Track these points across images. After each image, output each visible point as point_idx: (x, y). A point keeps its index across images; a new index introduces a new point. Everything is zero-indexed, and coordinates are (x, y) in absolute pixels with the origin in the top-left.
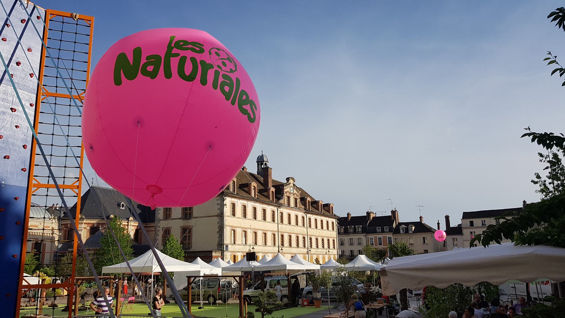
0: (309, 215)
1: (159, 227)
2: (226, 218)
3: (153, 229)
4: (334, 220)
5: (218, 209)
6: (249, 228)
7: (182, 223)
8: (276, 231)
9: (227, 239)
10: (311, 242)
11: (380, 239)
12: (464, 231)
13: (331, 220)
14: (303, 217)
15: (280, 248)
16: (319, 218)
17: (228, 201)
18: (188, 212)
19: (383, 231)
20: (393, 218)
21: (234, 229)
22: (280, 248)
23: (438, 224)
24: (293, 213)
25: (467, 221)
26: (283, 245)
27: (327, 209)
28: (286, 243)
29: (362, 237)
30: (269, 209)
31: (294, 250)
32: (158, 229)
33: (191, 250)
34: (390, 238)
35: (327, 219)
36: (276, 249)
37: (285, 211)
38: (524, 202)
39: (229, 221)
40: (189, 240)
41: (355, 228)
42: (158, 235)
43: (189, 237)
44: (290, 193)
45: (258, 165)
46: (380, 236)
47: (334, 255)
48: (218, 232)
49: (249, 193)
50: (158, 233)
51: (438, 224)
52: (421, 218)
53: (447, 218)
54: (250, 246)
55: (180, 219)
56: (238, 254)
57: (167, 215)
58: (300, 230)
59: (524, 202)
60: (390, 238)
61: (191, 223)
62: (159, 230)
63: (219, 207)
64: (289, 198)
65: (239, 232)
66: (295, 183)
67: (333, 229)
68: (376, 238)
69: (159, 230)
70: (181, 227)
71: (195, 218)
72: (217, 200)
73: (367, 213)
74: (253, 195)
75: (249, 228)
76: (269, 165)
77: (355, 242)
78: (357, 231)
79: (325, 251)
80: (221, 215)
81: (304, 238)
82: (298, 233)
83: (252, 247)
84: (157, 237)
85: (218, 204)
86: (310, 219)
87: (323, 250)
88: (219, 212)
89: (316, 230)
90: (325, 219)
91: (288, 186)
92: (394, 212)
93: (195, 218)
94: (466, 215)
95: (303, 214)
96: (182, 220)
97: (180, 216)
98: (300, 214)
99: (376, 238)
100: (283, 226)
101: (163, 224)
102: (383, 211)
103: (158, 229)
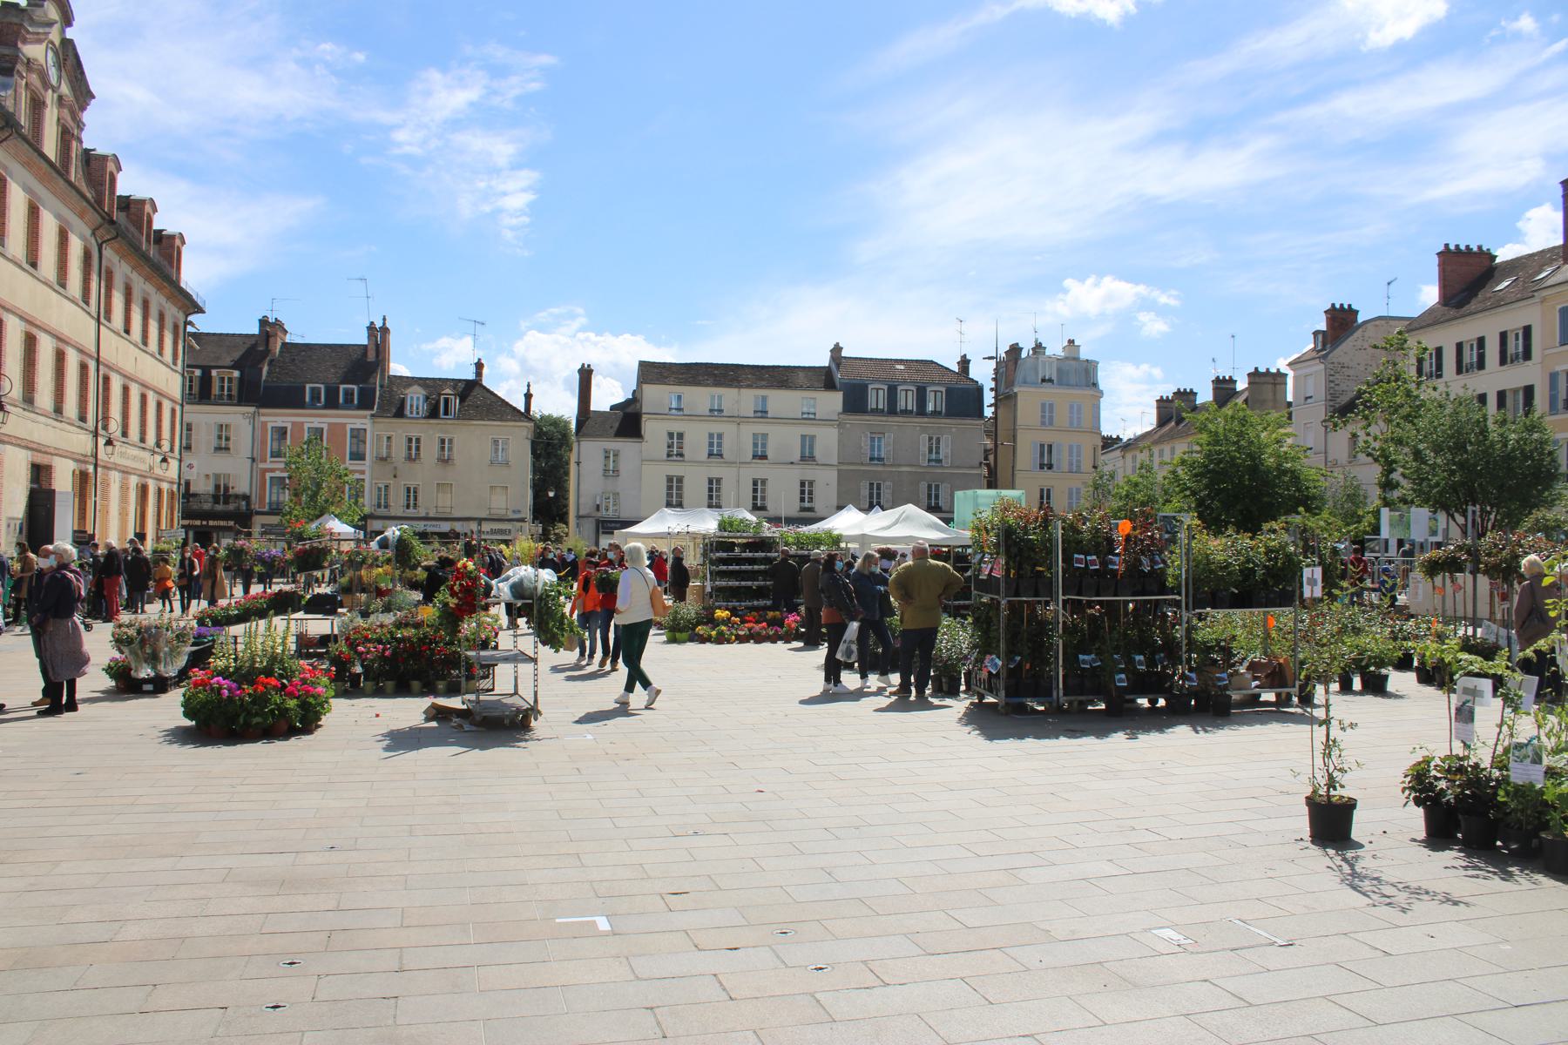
12: (649, 426)
19: (332, 403)
20: (371, 357)
25: (657, 395)
29: (238, 418)
34: (358, 435)
38: (837, 350)
51: (528, 396)
52: (479, 366)
53: (586, 375)
59: (837, 350)
60: (358, 435)
77: (204, 439)
78: (216, 390)
92: (379, 335)
94: (651, 372)
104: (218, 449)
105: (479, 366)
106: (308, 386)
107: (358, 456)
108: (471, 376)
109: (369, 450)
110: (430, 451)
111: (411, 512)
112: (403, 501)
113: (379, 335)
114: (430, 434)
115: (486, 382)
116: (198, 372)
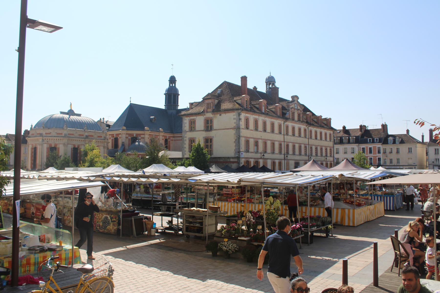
0: (310, 128)
1: (186, 137)
2: (242, 130)
3: (180, 138)
4: (332, 132)
5: (235, 123)
6: (260, 139)
7: (205, 134)
8: (282, 142)
9: (243, 148)
10: (312, 150)
11: (370, 148)
13: (329, 132)
14: (305, 130)
15: (286, 156)
16: (319, 130)
17: (243, 115)
18: (209, 125)
19: (373, 142)
21: (247, 139)
22: (286, 156)
23: (423, 136)
24: (297, 126)
26: (288, 153)
27: (325, 123)
28: (291, 152)
29: (355, 146)
30: (277, 122)
31: (297, 158)
32: (185, 139)
33: (213, 156)
35: (326, 131)
36: (282, 157)
37: (290, 124)
39: (244, 133)
40: (211, 148)
41: (349, 139)
42: (185, 144)
43: (211, 145)
44: (295, 109)
45: (267, 85)
46: (370, 146)
47: (331, 161)
48: (235, 142)
49: (259, 109)
50: (185, 142)
51: (423, 136)
52: (408, 131)
54: (261, 153)
55: (203, 131)
56: (251, 160)
57: (192, 128)
58: (302, 140)
60: (379, 148)
61: (211, 134)
62: (186, 140)
63: (235, 121)
64: (293, 113)
65: (252, 142)
66: (299, 100)
67: (330, 140)
68: (367, 147)
69: (186, 140)
70: (203, 138)
71: (216, 130)
72: (234, 115)
73: (361, 126)
74: (263, 111)
75: (260, 139)
76: (277, 85)
77: (349, 151)
78: (351, 141)
79: (323, 158)
80: (238, 128)
81: (306, 147)
82: (301, 142)
83: (262, 154)
84: (185, 146)
85: (234, 119)
86: (311, 131)
87: (322, 158)
88: (235, 125)
89: (316, 141)
90: (324, 131)
91: (293, 103)
92: (384, 127)
93: (216, 130)
95: (305, 127)
96: (204, 132)
97: (202, 128)
98: (303, 127)
99: (367, 147)
100: (289, 137)
101: (189, 135)
102: (373, 125)
103: (185, 139)
104: (352, 153)
105: (408, 131)
106: (368, 139)
107: (379, 152)
108: (405, 133)
109: (382, 151)
110: (394, 151)
111: (391, 164)
112: (389, 162)
113: (384, 127)
114: (394, 148)
115: (410, 134)
116: (347, 138)
